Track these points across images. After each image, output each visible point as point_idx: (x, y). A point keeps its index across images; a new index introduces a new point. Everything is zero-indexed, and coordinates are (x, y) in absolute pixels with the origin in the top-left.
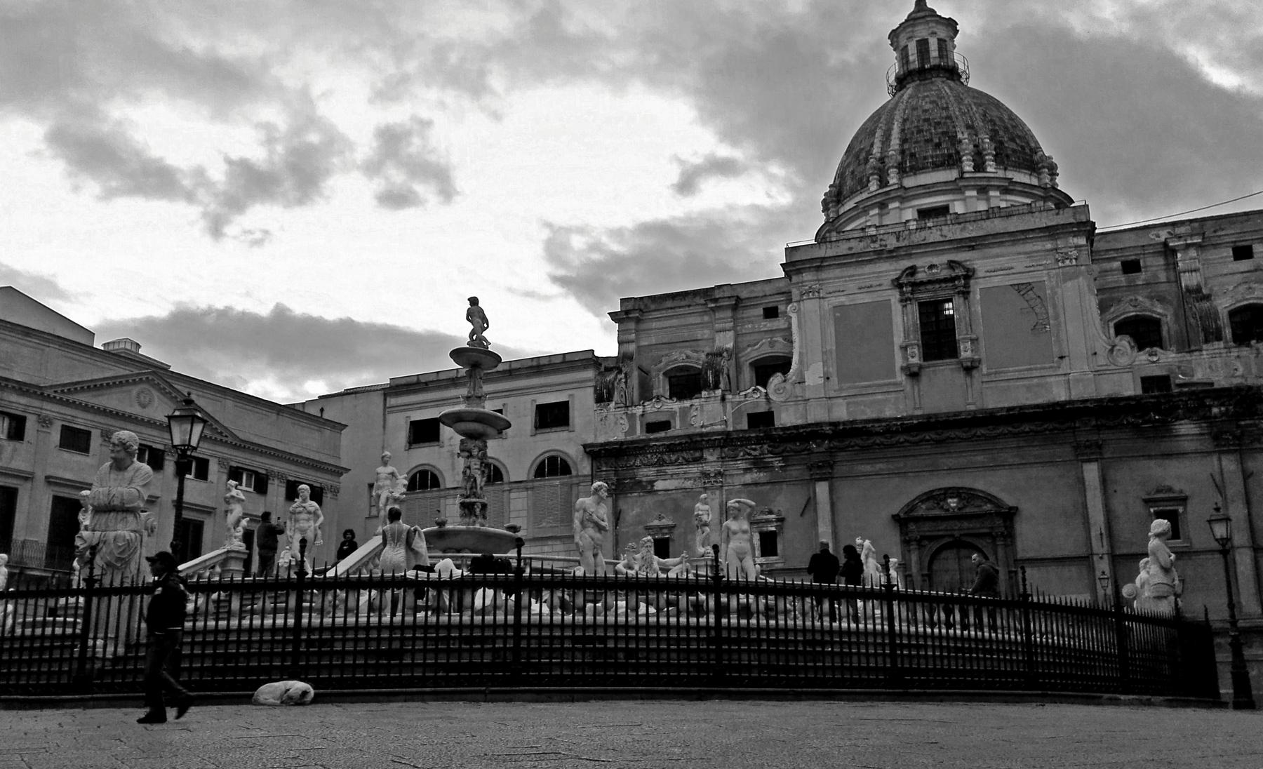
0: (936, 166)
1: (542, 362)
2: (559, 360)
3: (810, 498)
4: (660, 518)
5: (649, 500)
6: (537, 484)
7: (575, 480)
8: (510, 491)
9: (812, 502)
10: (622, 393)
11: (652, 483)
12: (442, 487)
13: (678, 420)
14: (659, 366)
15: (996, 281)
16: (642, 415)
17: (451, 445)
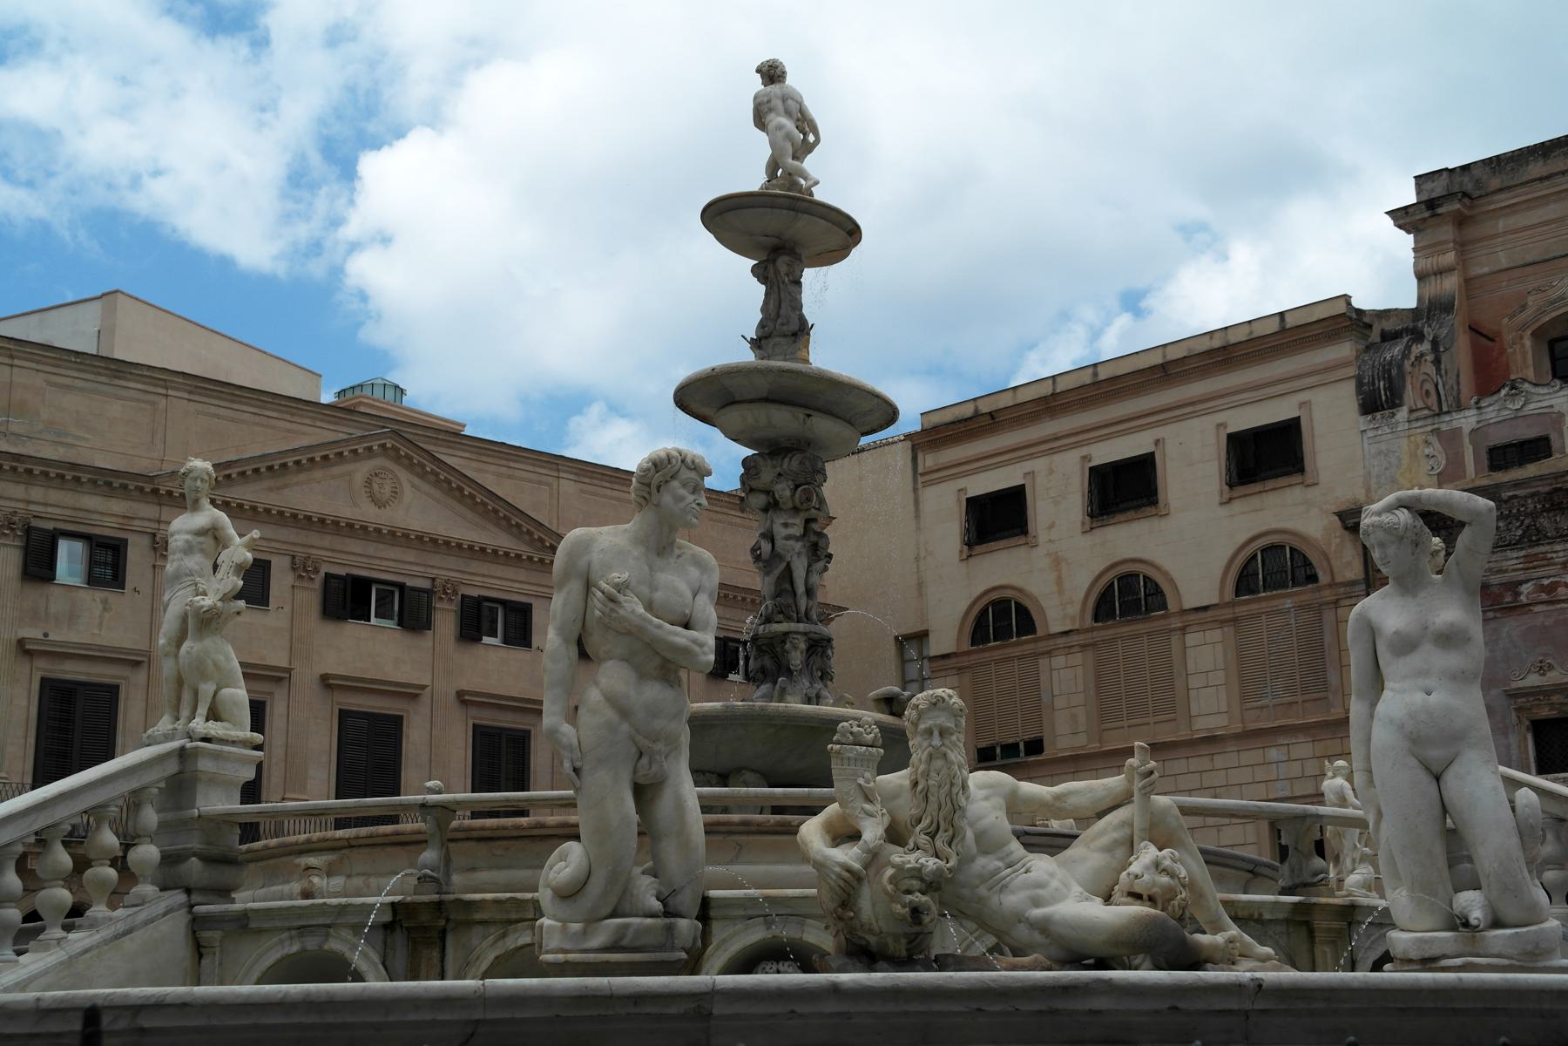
1: (1233, 339)
2: (1274, 326)
4: (1542, 669)
6: (1241, 610)
7: (1328, 595)
8: (1183, 630)
10: (1429, 386)
11: (1513, 587)
12: (1040, 633)
14: (1522, 317)
17: (1050, 541)
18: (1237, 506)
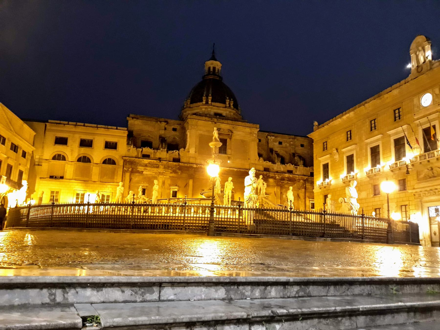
0: (220, 102)
3: (187, 183)
5: (141, 177)
9: (188, 184)
11: (142, 172)
13: (152, 155)
15: (238, 137)
16: (142, 151)
18: (105, 150)
